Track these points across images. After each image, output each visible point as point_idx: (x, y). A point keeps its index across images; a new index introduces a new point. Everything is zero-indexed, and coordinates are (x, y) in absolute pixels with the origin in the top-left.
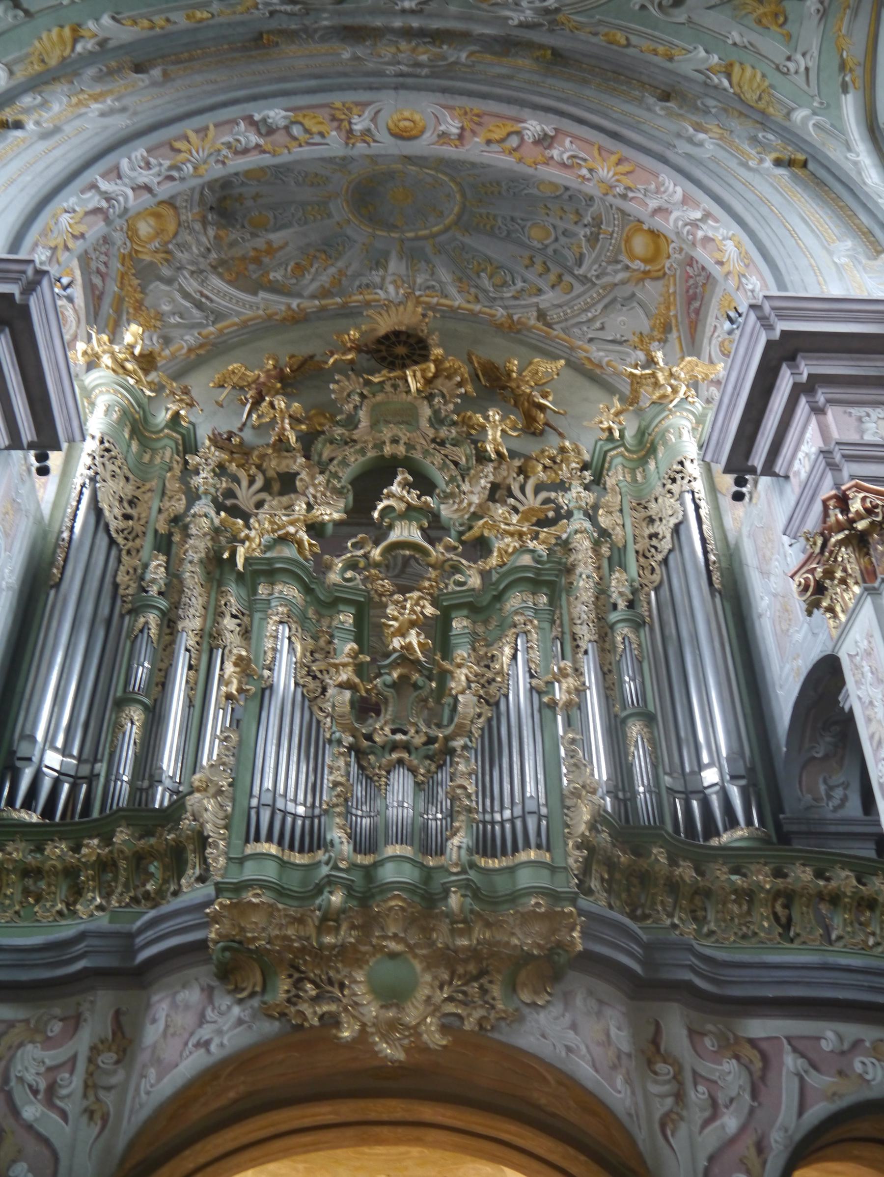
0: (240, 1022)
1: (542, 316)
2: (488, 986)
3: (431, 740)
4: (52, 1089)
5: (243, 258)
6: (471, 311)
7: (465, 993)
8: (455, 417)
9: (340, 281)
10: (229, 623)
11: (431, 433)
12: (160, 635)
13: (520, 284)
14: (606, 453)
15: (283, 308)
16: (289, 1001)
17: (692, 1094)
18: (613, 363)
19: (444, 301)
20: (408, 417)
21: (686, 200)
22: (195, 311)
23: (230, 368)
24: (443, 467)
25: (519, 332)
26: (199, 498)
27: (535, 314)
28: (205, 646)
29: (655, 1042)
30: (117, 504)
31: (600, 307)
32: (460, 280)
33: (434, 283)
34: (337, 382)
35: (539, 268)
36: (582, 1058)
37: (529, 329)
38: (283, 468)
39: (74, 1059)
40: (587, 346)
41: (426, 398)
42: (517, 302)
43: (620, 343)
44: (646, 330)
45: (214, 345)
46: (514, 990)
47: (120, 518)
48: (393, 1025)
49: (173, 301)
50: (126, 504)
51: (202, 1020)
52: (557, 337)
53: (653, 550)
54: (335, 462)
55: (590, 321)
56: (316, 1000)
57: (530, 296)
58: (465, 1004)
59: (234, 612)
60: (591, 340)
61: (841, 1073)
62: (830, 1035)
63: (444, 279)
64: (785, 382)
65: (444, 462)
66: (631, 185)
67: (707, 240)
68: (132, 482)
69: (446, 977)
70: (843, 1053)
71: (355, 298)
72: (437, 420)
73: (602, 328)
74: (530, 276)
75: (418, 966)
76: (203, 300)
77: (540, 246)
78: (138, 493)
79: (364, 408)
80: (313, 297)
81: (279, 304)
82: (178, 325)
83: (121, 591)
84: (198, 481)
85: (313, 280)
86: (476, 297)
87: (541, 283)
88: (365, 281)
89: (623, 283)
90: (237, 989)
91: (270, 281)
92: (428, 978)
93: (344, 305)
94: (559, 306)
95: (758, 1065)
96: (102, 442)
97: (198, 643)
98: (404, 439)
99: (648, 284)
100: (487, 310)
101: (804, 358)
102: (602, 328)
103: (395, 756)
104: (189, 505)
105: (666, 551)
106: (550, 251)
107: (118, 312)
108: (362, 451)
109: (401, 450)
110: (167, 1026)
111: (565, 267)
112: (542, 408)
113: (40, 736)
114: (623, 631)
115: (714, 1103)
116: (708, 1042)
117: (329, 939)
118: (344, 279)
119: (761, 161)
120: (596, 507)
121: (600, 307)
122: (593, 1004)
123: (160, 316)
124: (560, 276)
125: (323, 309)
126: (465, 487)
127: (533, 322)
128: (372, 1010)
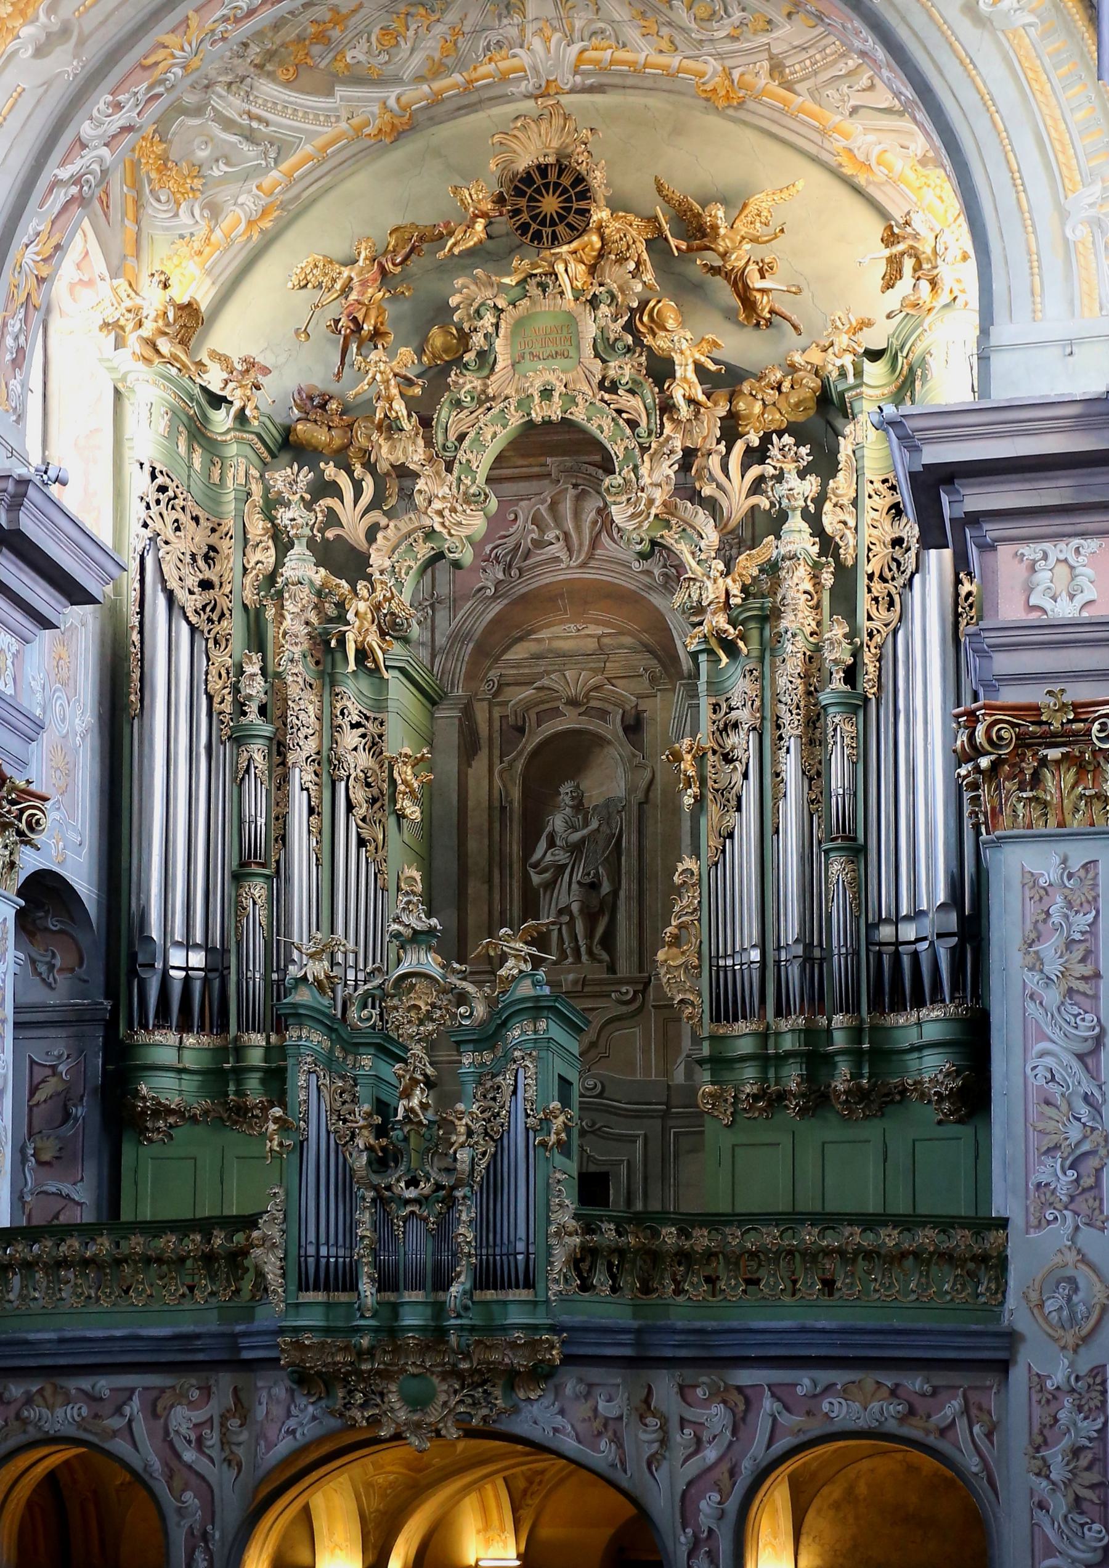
1: (777, 68)
2: (490, 1389)
3: (439, 1187)
4: (200, 1440)
5: (300, 39)
7: (472, 1396)
9: (455, 44)
10: (351, 738)
12: (270, 770)
13: (737, 15)
15: (376, 109)
16: (345, 1405)
17: (678, 1438)
18: (888, 156)
19: (621, 55)
22: (245, 146)
25: (741, 104)
27: (766, 65)
28: (325, 777)
29: (647, 1401)
30: (186, 570)
33: (602, 25)
36: (568, 1435)
38: (398, 457)
41: (591, 302)
42: (736, 46)
45: (282, 206)
46: (512, 1388)
47: (197, 590)
48: (418, 1425)
49: (209, 140)
50: (201, 563)
52: (801, 110)
53: (894, 566)
54: (466, 443)
55: (850, 74)
56: (363, 1407)
57: (755, 32)
58: (474, 1404)
59: (355, 719)
60: (854, 110)
61: (809, 1413)
62: (806, 1381)
63: (617, 17)
65: (617, 424)
69: (457, 1387)
70: (815, 1396)
71: (484, 70)
72: (604, 348)
75: (435, 1380)
76: (255, 125)
78: (214, 540)
79: (502, 332)
80: (419, 79)
82: (225, 178)
83: (216, 706)
84: (284, 516)
85: (413, 50)
90: (309, 1394)
91: (347, 66)
92: (445, 1387)
95: (742, 1407)
96: (153, 477)
97: (316, 774)
103: (409, 1209)
104: (279, 563)
105: (909, 572)
107: (136, 185)
109: (554, 411)
112: (763, 291)
113: (155, 933)
114: (835, 717)
115: (699, 1443)
116: (699, 1392)
117: (365, 1367)
118: (461, 39)
120: (820, 499)
122: (582, 1388)
123: (198, 170)
125: (436, 100)
126: (644, 470)
127: (763, 81)
128: (402, 1415)
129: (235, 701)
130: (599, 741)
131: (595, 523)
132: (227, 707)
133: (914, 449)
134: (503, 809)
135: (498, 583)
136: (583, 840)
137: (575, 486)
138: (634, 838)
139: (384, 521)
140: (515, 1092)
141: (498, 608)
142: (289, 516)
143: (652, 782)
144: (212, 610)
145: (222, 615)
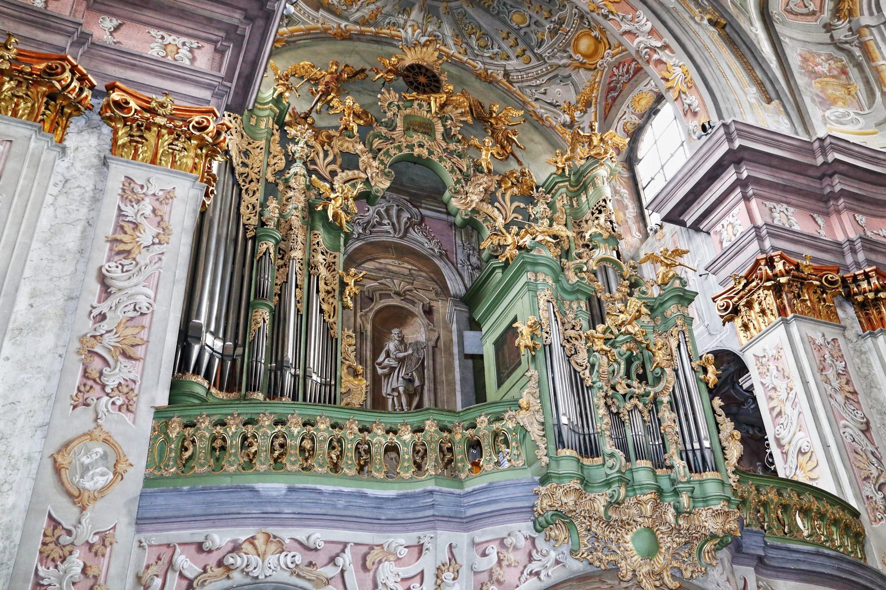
0: (557, 562)
1: (507, 74)
6: (461, 60)
8: (460, 137)
11: (444, 145)
14: (556, 183)
15: (335, 26)
20: (427, 129)
21: (652, 32)
23: (302, 64)
24: (452, 171)
26: (294, 161)
31: (546, 78)
32: (457, 36)
34: (382, 94)
35: (511, 41)
37: (498, 82)
39: (422, 573)
40: (533, 103)
41: (440, 118)
42: (491, 61)
43: (555, 106)
44: (573, 102)
45: (286, 42)
51: (530, 559)
52: (515, 92)
54: (382, 152)
55: (537, 86)
57: (501, 59)
60: (537, 100)
64: (729, 177)
66: (613, 10)
67: (660, 61)
68: (245, 138)
71: (384, 31)
73: (545, 93)
74: (504, 46)
77: (516, 27)
78: (249, 148)
80: (356, 22)
81: (333, 23)
84: (292, 147)
85: (358, 10)
86: (465, 51)
87: (510, 52)
88: (393, 20)
89: (565, 66)
93: (376, 34)
94: (519, 71)
98: (427, 145)
99: (582, 71)
100: (469, 61)
101: (746, 165)
102: (545, 93)
106: (522, 32)
108: (399, 148)
109: (425, 153)
110: (500, 561)
111: (529, 45)
119: (702, 18)
121: (546, 78)
124: (524, 51)
125: (362, 33)
127: (500, 78)
129: (260, 220)
130: (413, 315)
131: (406, 223)
132: (254, 221)
133: (730, 140)
134: (362, 333)
135: (359, 234)
136: (404, 358)
137: (398, 206)
138: (431, 363)
139: (339, 170)
140: (679, 346)
141: (360, 244)
142: (297, 149)
143: (438, 338)
144: (246, 177)
145: (252, 181)
